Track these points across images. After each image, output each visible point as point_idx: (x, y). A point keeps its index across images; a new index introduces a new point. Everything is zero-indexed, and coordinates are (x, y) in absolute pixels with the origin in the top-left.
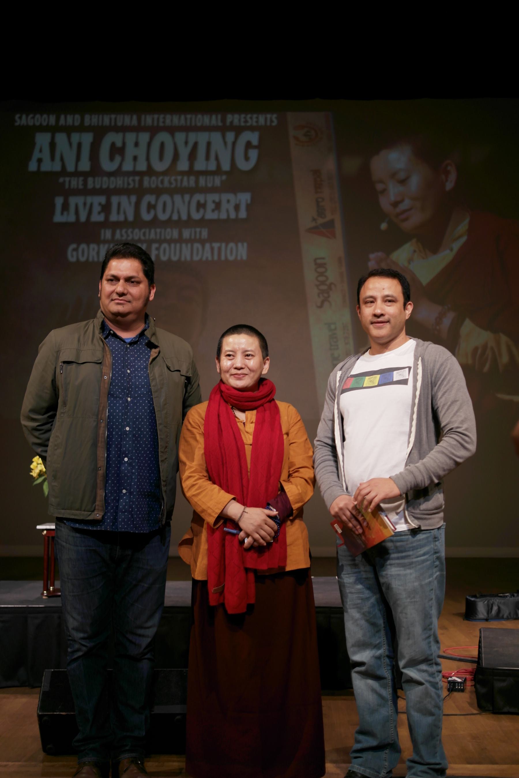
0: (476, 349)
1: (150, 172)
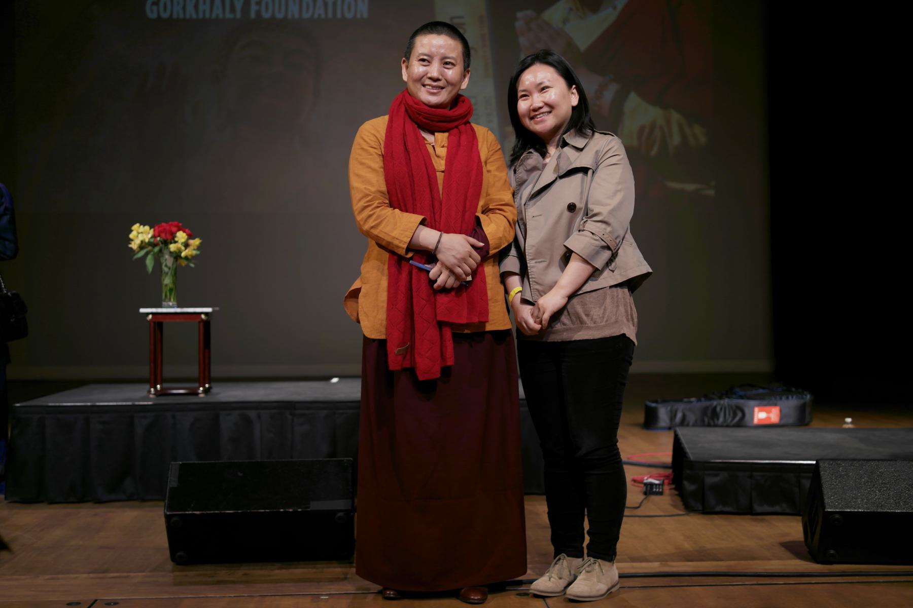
0: (642, 128)
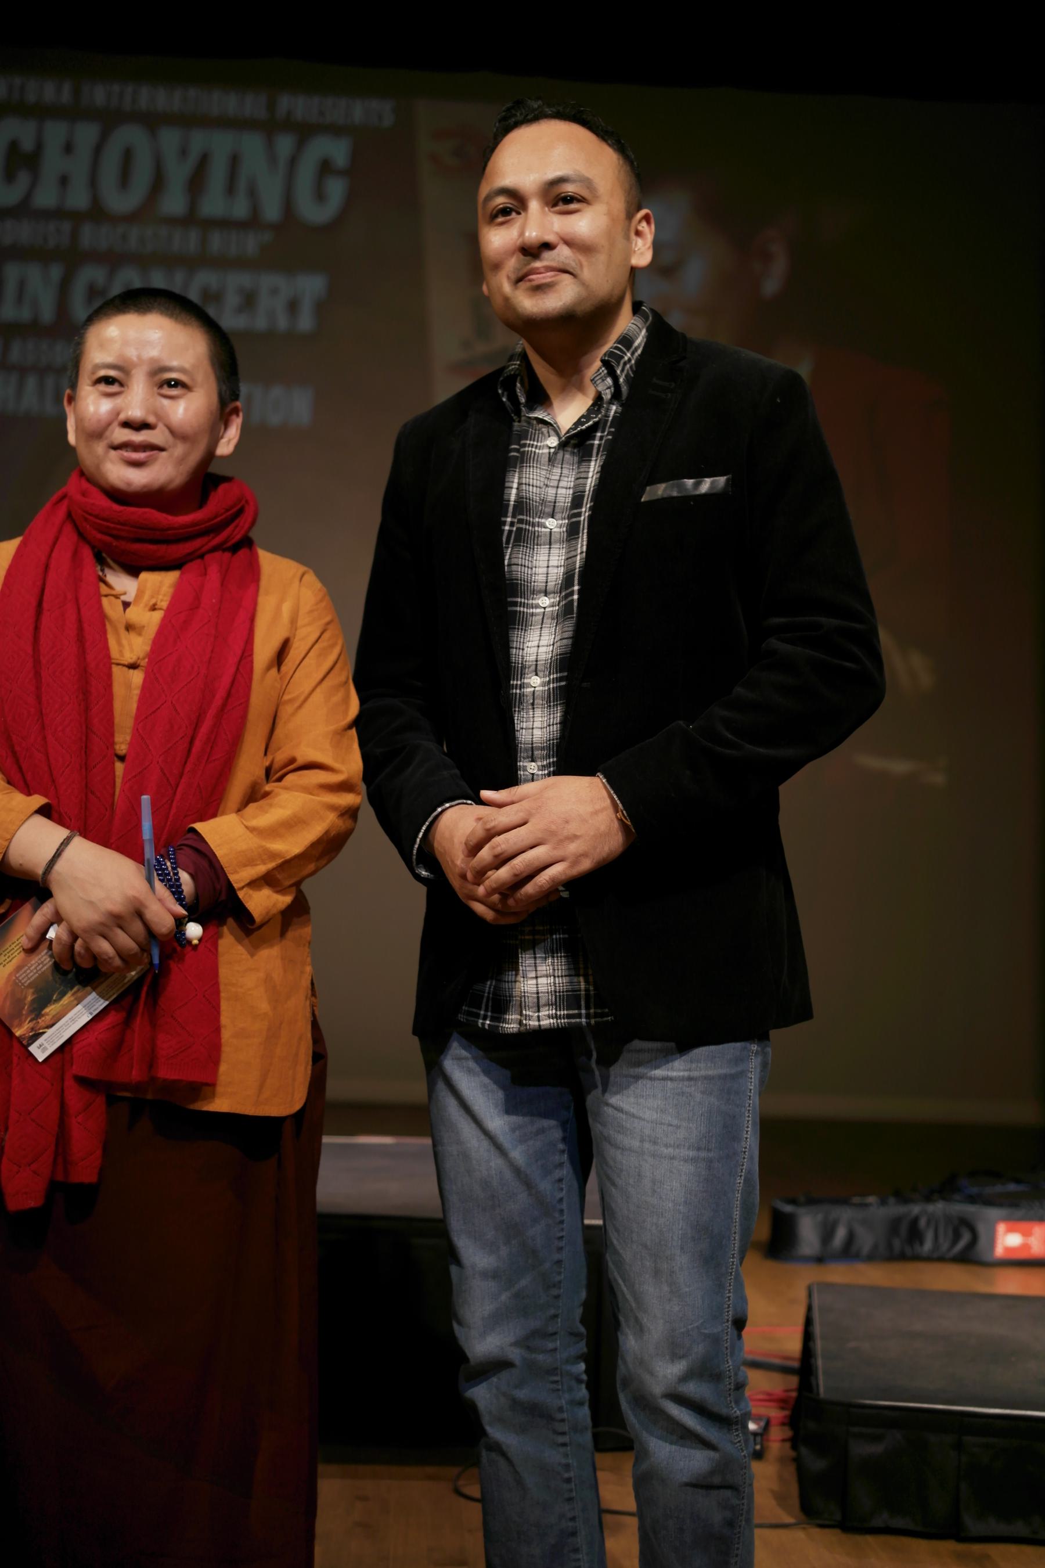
1: (97, 213)
